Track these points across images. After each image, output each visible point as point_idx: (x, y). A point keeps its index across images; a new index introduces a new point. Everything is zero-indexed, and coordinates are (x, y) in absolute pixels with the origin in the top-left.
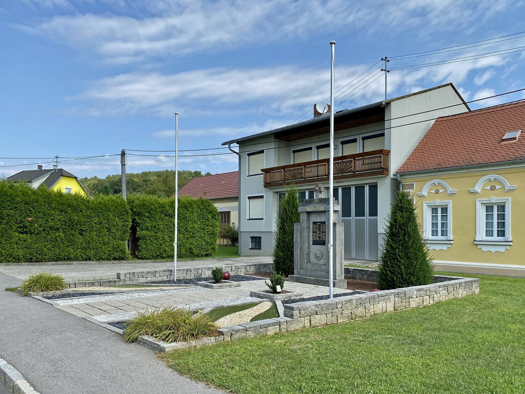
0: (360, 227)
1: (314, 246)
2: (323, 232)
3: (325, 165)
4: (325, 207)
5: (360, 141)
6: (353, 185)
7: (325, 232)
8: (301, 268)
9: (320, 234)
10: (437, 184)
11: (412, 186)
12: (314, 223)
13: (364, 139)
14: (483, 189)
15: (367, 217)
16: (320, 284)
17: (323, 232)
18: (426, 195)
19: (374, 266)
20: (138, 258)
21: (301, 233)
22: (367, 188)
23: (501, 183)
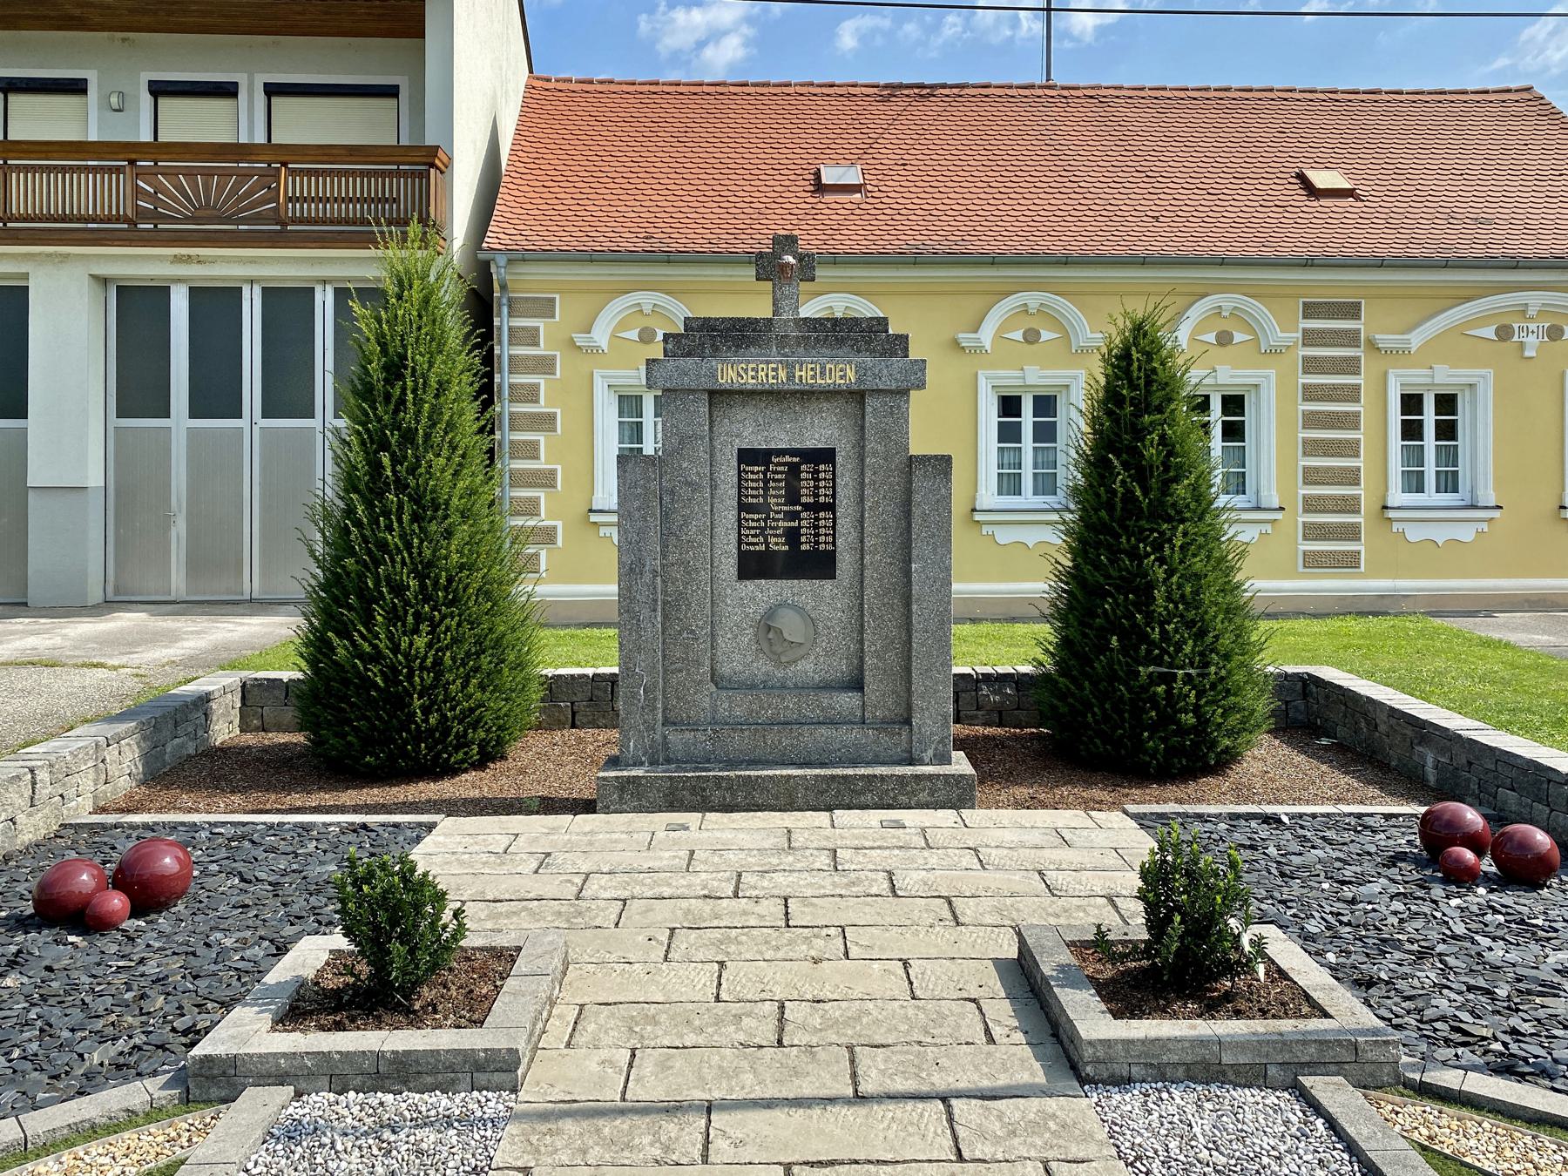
0: (212, 465)
1: (750, 586)
2: (815, 507)
3: (118, 170)
4: (861, 371)
5: (252, 100)
6: (179, 280)
7: (831, 507)
8: (666, 722)
9: (794, 516)
10: (647, 309)
11: (545, 308)
12: (747, 457)
13: (272, 90)
14: (999, 336)
15: (252, 422)
16: (868, 798)
17: (815, 507)
18: (604, 344)
19: (265, 640)
20: (1083, 1081)
21: (666, 516)
22: (324, 301)
23: (1056, 322)
